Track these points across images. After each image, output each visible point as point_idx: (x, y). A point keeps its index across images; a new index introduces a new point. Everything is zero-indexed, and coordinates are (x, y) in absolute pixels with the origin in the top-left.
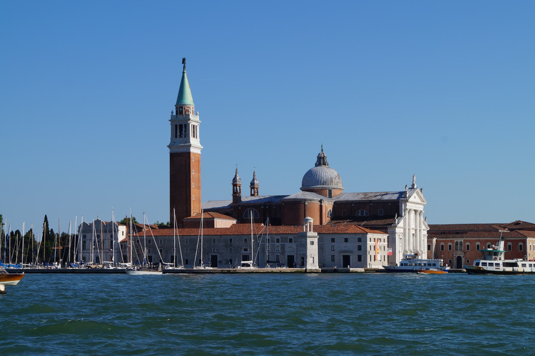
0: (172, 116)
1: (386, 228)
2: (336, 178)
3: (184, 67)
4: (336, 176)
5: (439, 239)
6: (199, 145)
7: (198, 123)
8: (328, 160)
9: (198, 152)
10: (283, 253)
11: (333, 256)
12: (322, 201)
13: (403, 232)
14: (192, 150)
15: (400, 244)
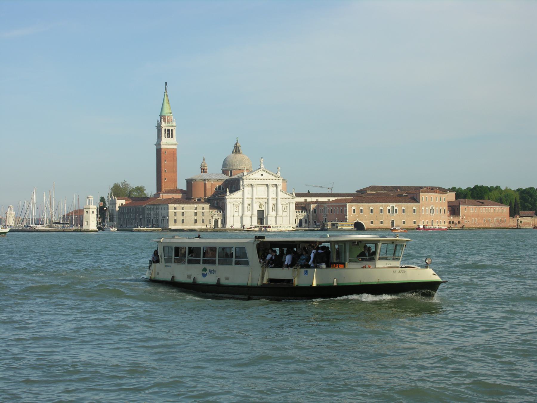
0: (158, 123)
1: (224, 199)
2: (237, 162)
3: (166, 89)
4: (238, 160)
5: (319, 205)
6: (176, 142)
7: (174, 127)
8: (241, 149)
9: (175, 147)
10: (150, 218)
11: (161, 220)
12: (206, 180)
13: (242, 202)
14: (163, 147)
15: (237, 210)
